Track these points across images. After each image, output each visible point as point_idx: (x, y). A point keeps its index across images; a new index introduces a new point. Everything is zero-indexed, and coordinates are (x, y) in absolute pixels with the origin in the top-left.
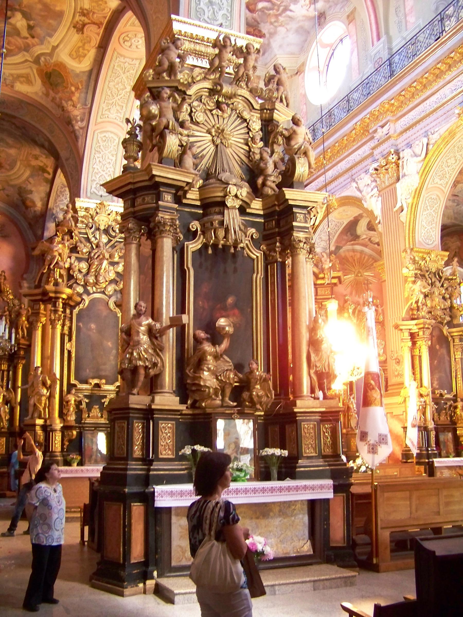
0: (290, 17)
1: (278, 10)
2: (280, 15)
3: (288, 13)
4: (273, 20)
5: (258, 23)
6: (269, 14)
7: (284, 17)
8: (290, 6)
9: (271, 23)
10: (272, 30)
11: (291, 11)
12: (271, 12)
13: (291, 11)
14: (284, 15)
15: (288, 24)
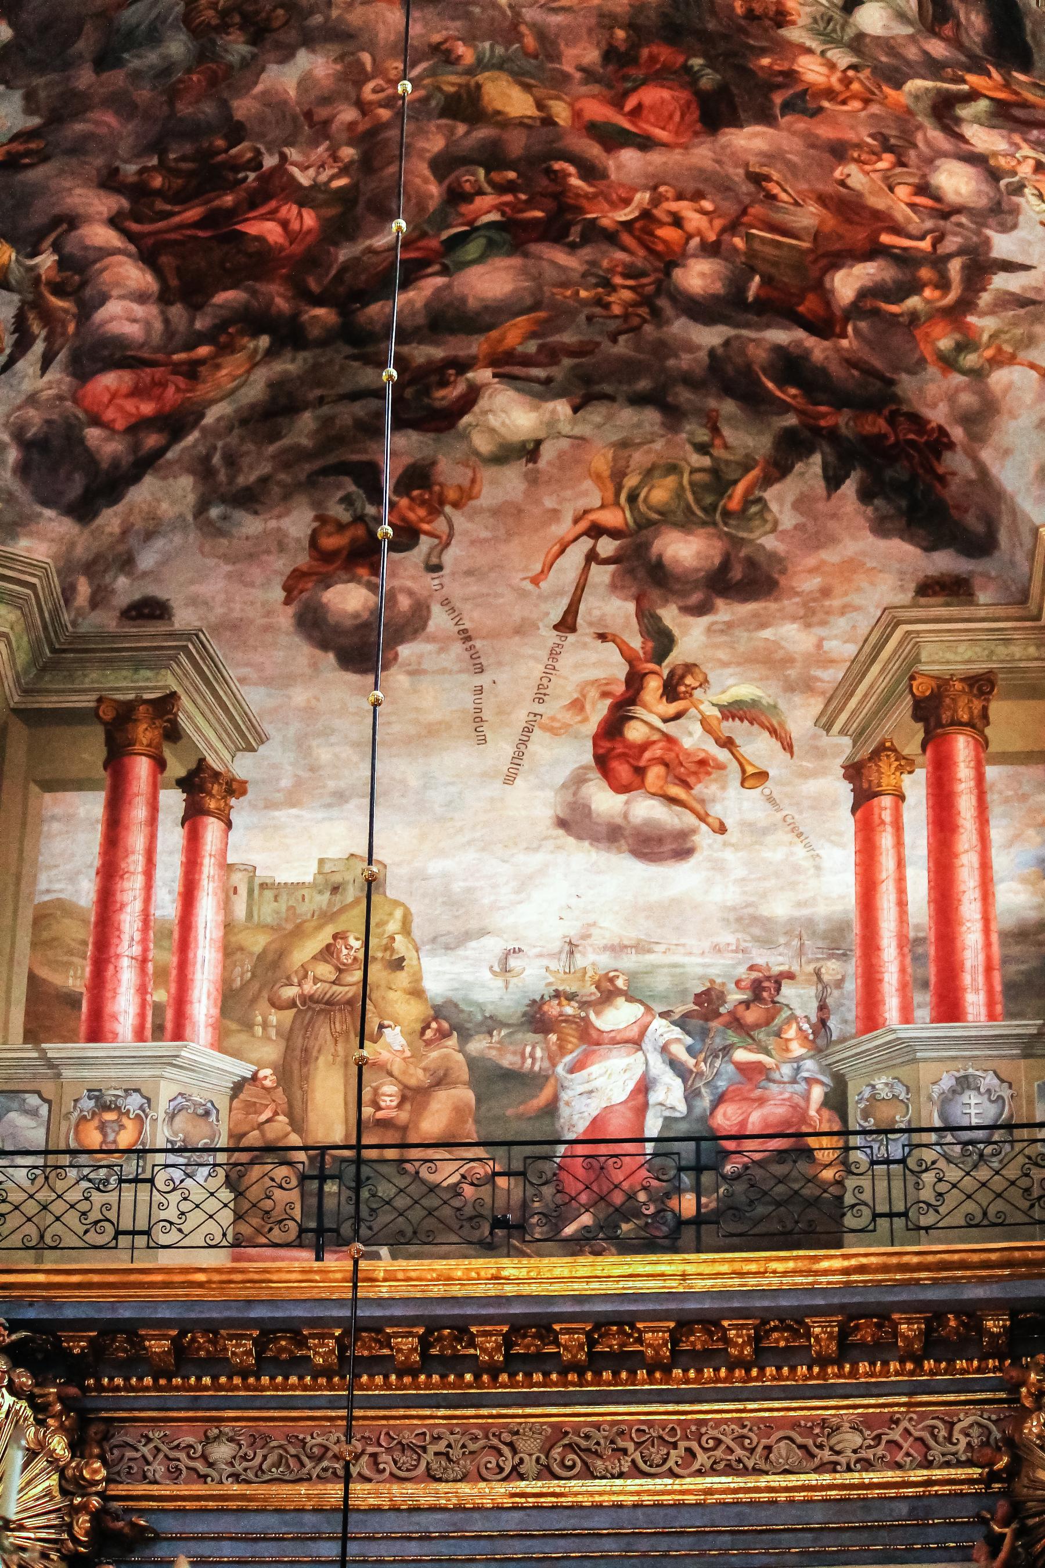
0: (1021, 301)
1: (943, 284)
2: (966, 304)
3: (1001, 281)
4: (945, 344)
5: (891, 383)
6: (914, 317)
7: (992, 311)
8: (987, 242)
9: (948, 363)
10: (967, 399)
11: (1009, 266)
12: (914, 302)
13: (1009, 266)
14: (985, 299)
15: (1030, 341)
